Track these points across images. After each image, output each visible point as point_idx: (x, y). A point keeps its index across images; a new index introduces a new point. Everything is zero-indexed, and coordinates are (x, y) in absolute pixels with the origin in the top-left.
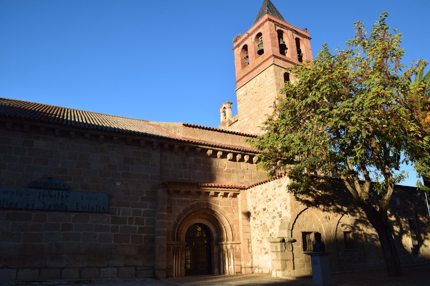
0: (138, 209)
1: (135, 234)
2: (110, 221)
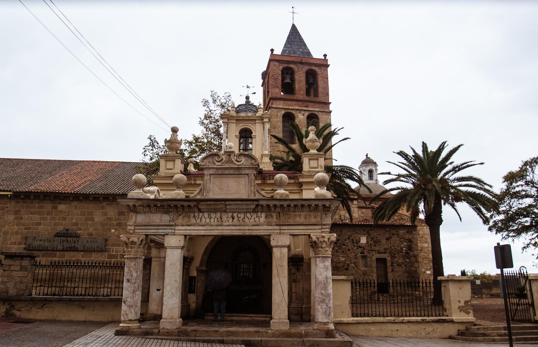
2: (106, 257)
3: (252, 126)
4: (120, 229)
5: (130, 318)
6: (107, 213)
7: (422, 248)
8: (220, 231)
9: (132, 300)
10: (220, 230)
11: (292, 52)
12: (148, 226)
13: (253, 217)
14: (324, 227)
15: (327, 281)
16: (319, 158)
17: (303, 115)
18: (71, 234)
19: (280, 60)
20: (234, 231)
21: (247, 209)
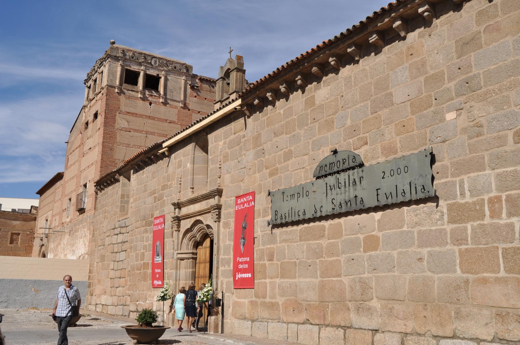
0: (509, 169)
1: (511, 245)
2: (446, 217)
4: (473, 103)
6: (424, 64)
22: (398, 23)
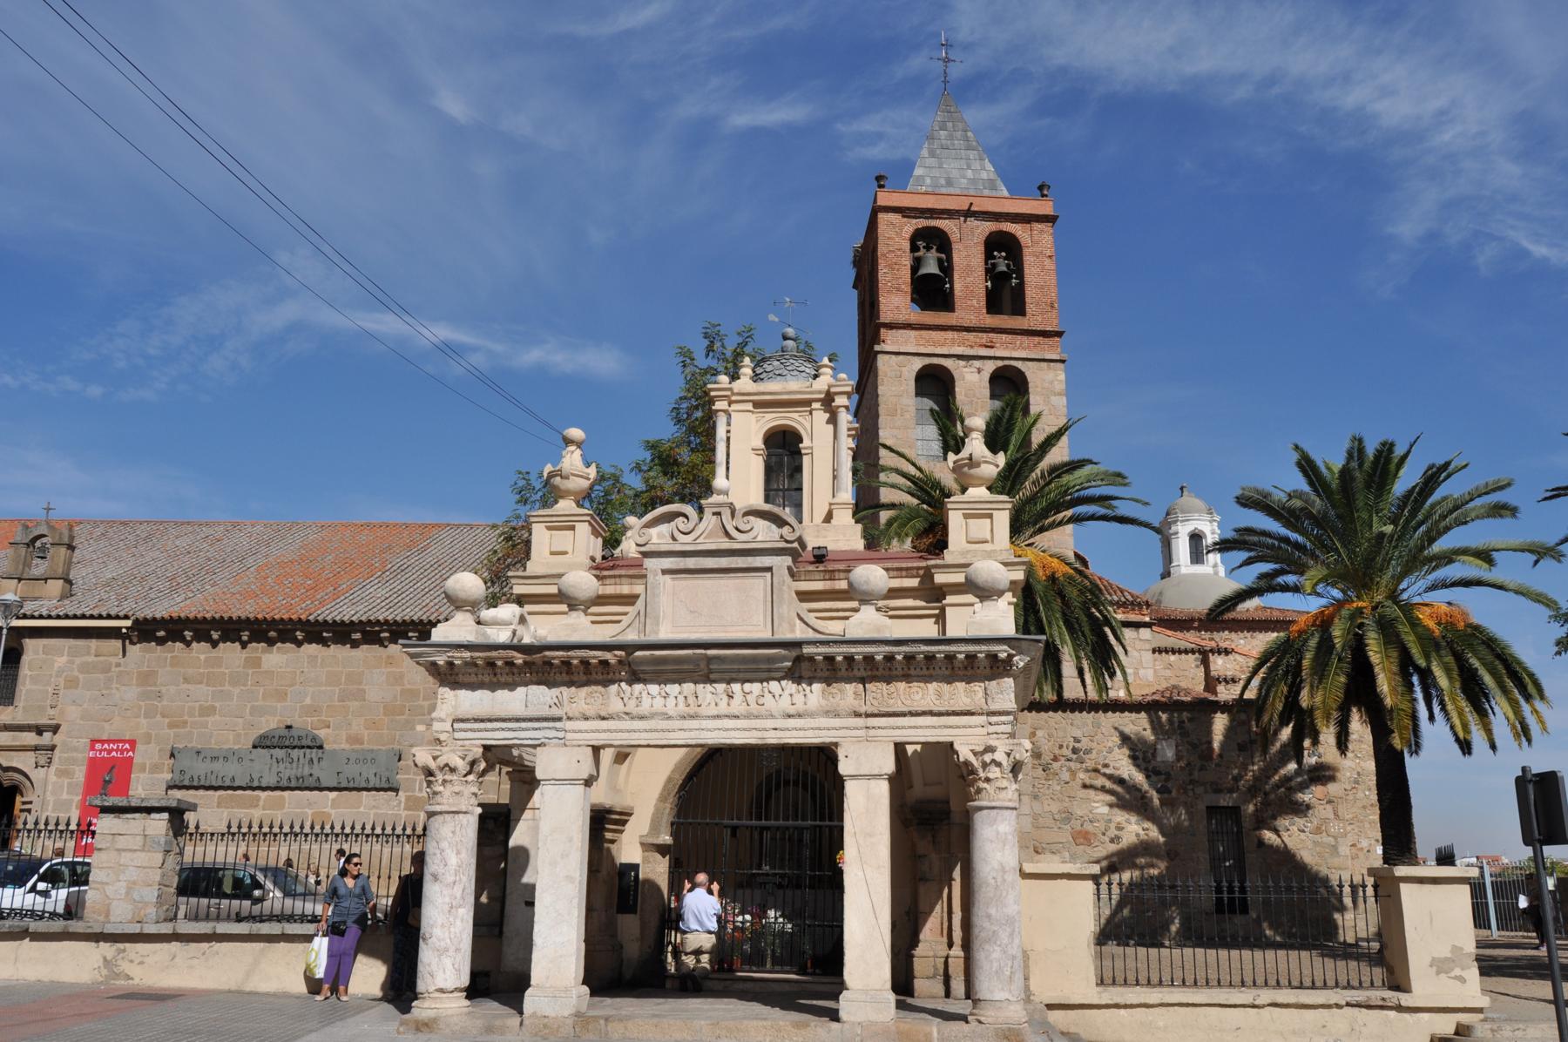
2: (403, 805)
3: (800, 419)
5: (441, 985)
6: (402, 676)
7: (1359, 774)
8: (692, 734)
9: (447, 934)
10: (691, 730)
11: (943, 182)
12: (490, 720)
13: (787, 692)
14: (994, 719)
15: (1004, 880)
16: (995, 513)
17: (979, 371)
18: (300, 738)
19: (908, 209)
20: (733, 734)
21: (769, 670)
22: (387, 635)
